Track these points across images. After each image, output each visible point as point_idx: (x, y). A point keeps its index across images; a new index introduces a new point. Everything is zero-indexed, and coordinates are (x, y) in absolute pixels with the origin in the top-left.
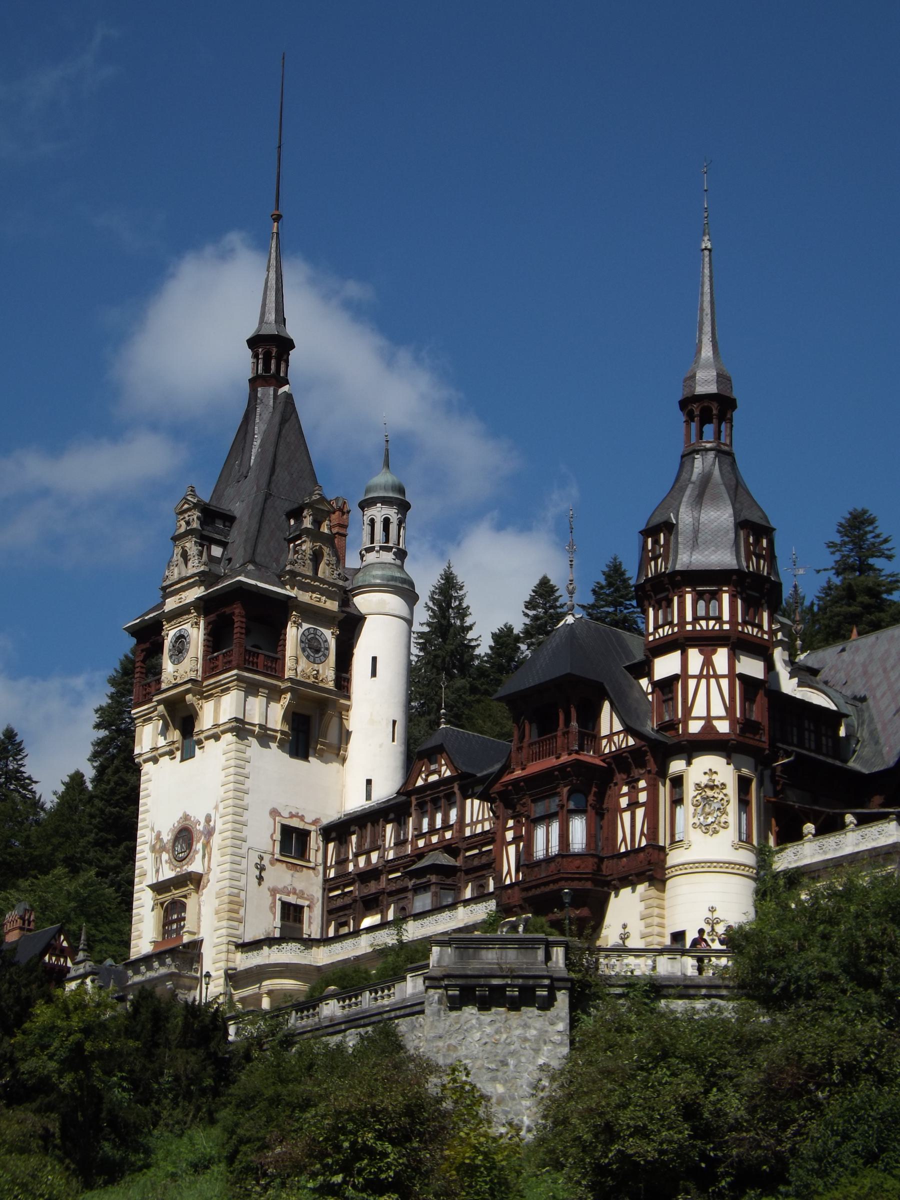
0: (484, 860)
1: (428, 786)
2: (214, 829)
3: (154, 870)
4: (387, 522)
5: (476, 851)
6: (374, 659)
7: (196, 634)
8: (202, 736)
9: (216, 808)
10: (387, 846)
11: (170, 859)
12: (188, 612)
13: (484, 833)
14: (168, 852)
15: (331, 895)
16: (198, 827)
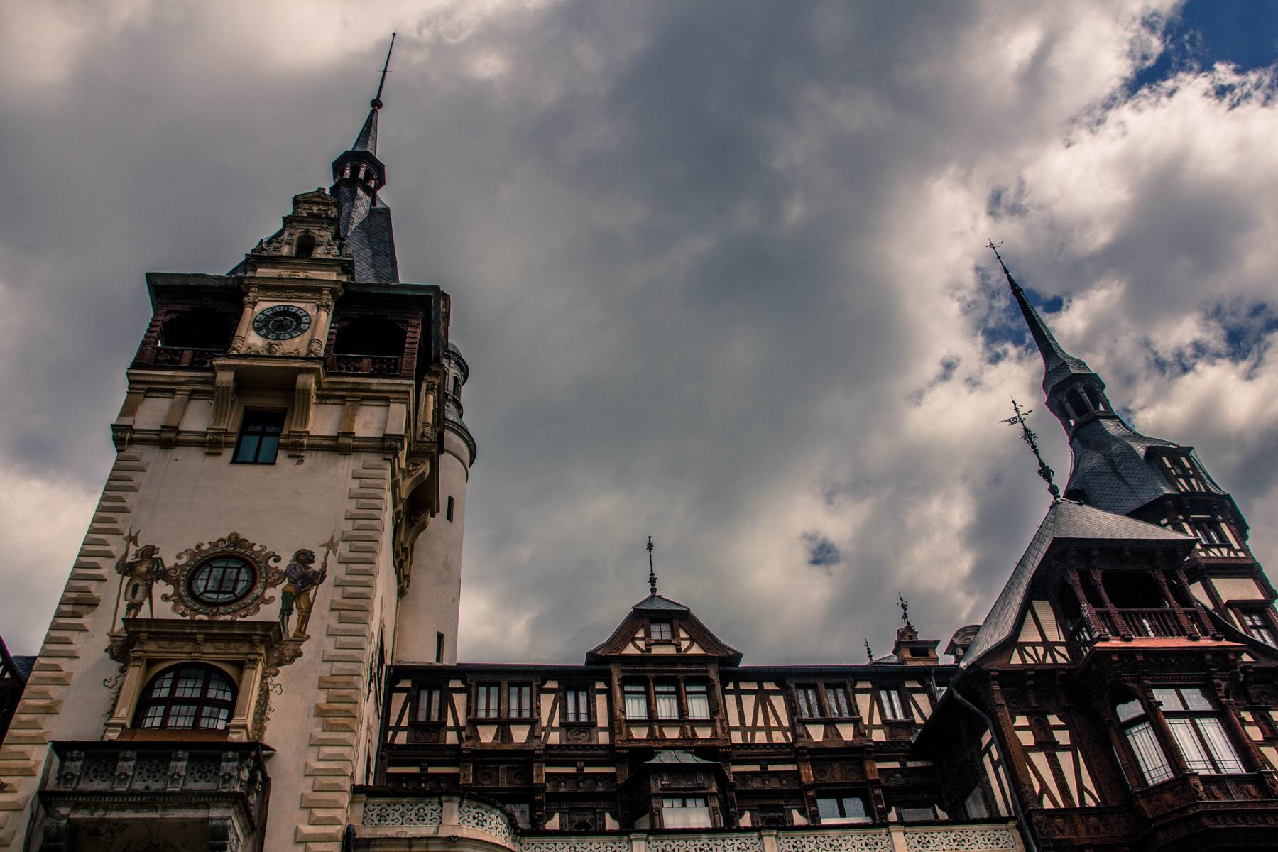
0: (774, 785)
1: (644, 659)
2: (321, 576)
3: (123, 605)
4: (456, 380)
5: (756, 768)
6: (451, 500)
7: (323, 323)
8: (305, 441)
9: (331, 546)
10: (544, 723)
11: (177, 593)
12: (319, 290)
13: (772, 745)
14: (175, 583)
15: (391, 770)
16: (271, 563)
